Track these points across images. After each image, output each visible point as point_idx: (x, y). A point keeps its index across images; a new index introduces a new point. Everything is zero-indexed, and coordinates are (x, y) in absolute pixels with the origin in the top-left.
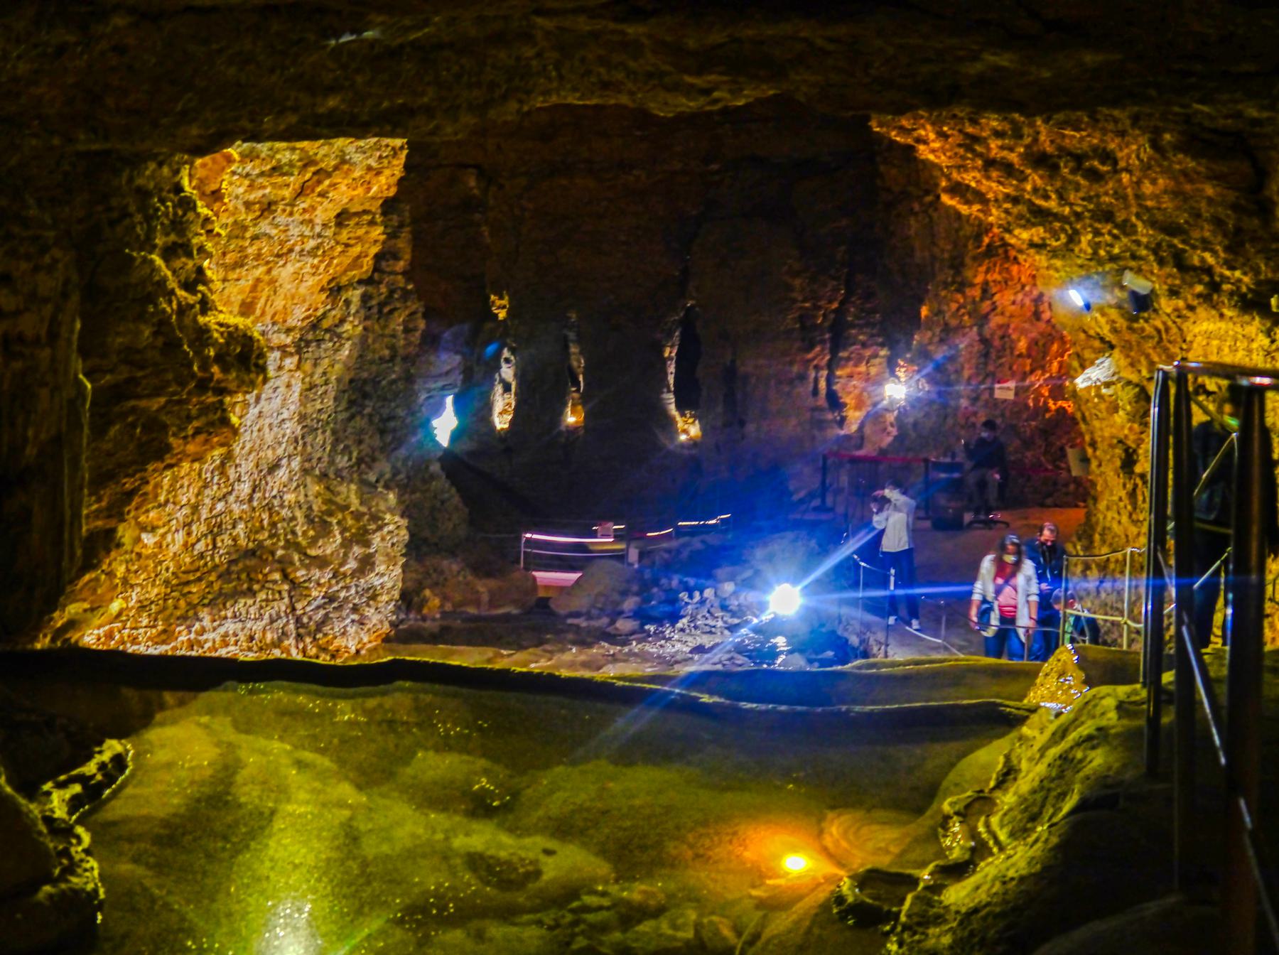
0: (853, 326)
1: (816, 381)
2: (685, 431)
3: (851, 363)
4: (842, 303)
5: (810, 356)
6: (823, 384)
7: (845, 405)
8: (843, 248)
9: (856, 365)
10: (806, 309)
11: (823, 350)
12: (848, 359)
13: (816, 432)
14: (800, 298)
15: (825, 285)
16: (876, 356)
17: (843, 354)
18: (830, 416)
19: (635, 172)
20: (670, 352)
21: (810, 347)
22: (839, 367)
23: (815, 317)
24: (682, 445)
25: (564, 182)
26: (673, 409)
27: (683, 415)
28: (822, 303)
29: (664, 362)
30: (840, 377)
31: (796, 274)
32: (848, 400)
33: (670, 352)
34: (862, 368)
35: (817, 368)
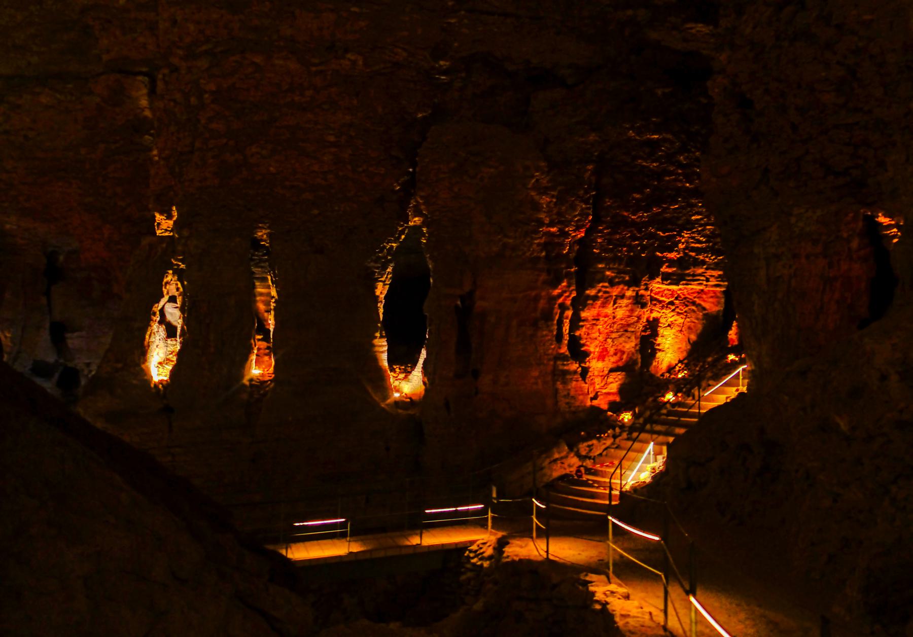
1: (560, 323)
3: (599, 302)
5: (557, 292)
6: (566, 328)
7: (587, 354)
8: (590, 167)
9: (604, 305)
10: (553, 235)
11: (569, 286)
12: (595, 298)
13: (559, 385)
14: (547, 221)
16: (623, 297)
17: (592, 292)
18: (575, 366)
19: (349, 56)
21: (555, 283)
22: (584, 306)
23: (562, 245)
24: (397, 403)
25: (258, 60)
30: (586, 320)
31: (544, 191)
32: (593, 348)
34: (609, 310)
35: (563, 307)
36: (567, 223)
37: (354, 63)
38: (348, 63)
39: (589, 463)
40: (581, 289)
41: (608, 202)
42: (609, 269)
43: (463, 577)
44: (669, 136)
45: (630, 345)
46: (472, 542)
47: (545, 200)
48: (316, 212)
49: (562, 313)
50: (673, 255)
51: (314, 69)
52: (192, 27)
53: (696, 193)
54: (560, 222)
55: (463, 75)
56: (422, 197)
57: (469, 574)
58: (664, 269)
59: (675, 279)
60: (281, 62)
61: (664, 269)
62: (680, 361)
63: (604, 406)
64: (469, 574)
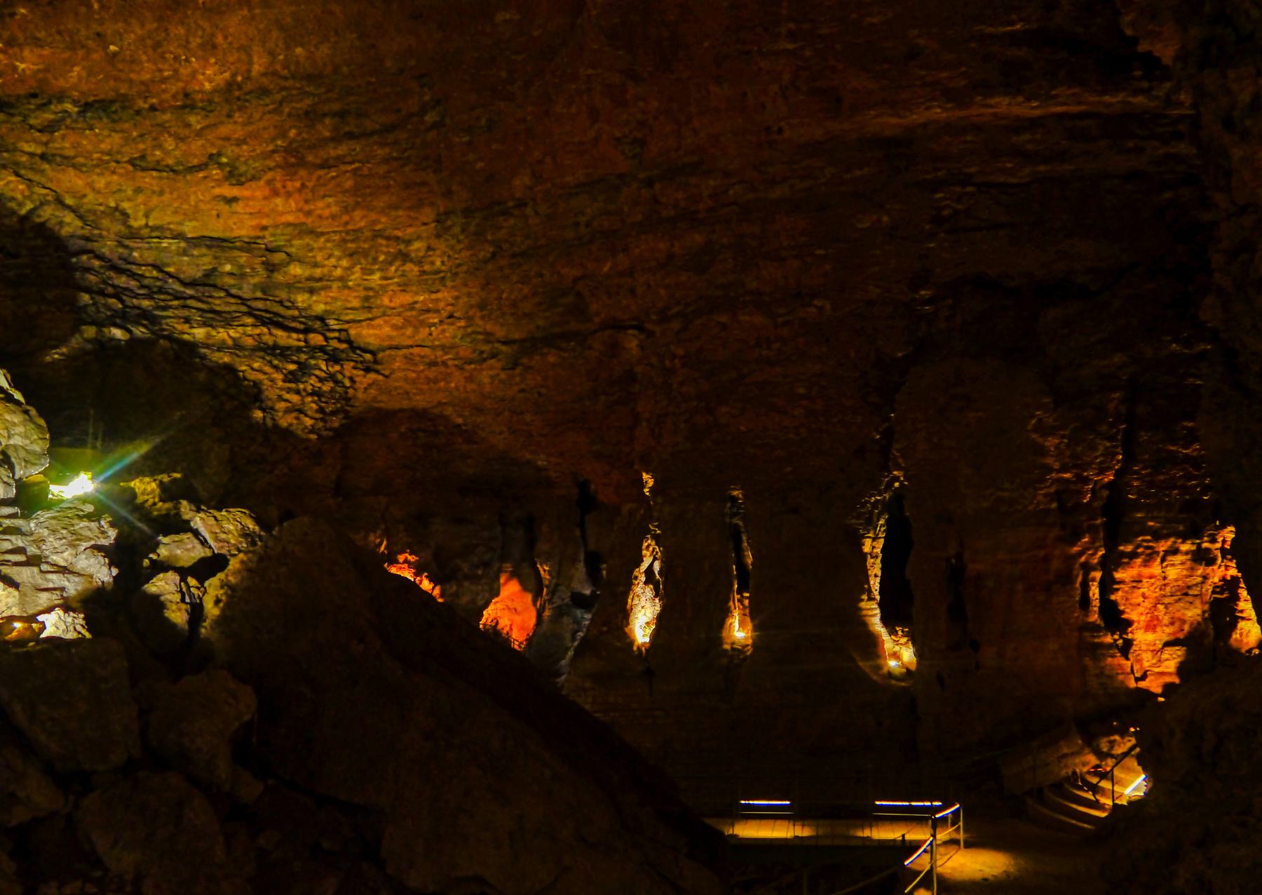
0: (1136, 506)
1: (1085, 587)
2: (896, 656)
3: (1139, 561)
4: (1118, 474)
5: (1076, 549)
6: (1095, 591)
7: (1129, 623)
8: (1117, 395)
9: (1146, 563)
10: (1067, 480)
11: (1093, 541)
12: (1134, 555)
13: (1088, 661)
14: (1057, 466)
15: (1093, 448)
16: (1175, 551)
19: (816, 302)
20: (873, 546)
21: (1075, 537)
22: (1118, 565)
23: (1081, 494)
25: (724, 319)
26: (876, 623)
27: (892, 632)
28: (1089, 473)
29: (864, 556)
30: (1122, 582)
33: (873, 546)
34: (1156, 569)
35: (1087, 568)
36: (1087, 466)
37: (821, 309)
38: (814, 310)
41: (1144, 436)
42: (1152, 519)
47: (1051, 442)
48: (789, 469)
49: (1086, 576)
52: (662, 292)
54: (1075, 466)
56: (898, 450)
60: (747, 318)
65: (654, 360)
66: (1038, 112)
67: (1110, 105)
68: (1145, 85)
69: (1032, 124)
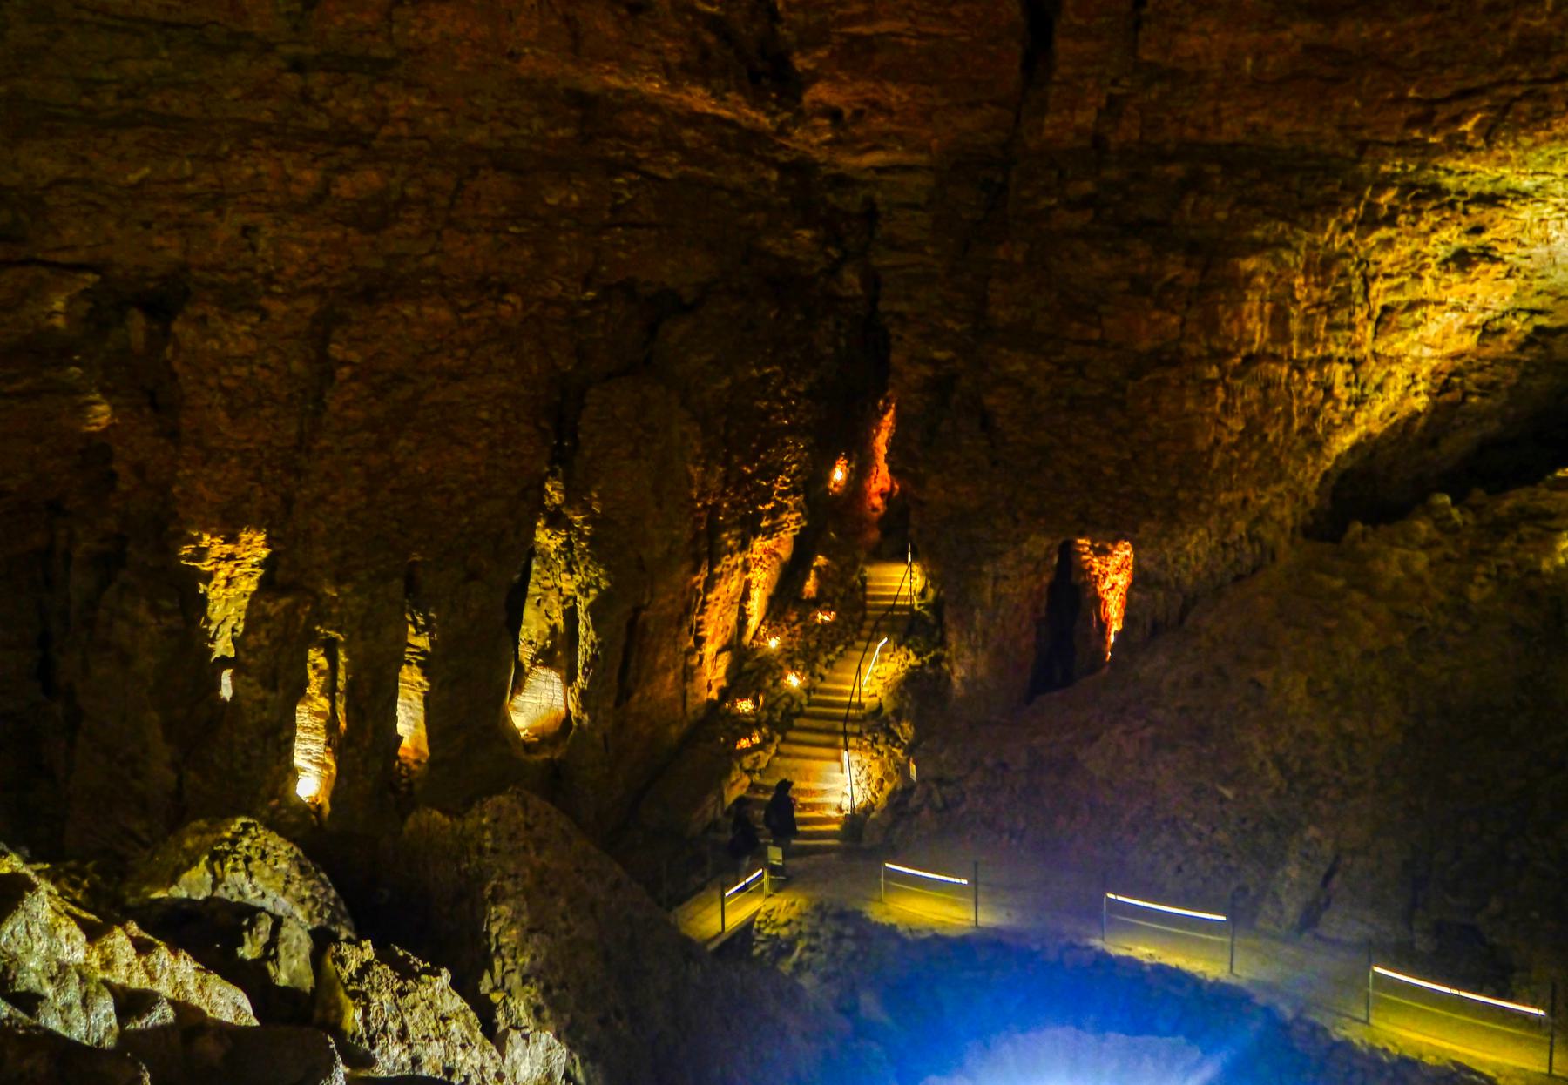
0: (724, 528)
16: (736, 567)
25: (408, 311)
35: (698, 595)
38: (509, 309)
39: (757, 778)
40: (710, 570)
42: (730, 537)
43: (756, 952)
44: (777, 368)
45: (732, 619)
46: (757, 912)
50: (768, 507)
51: (465, 317)
53: (790, 430)
55: (606, 307)
56: (599, 492)
57: (763, 947)
58: (765, 524)
59: (769, 533)
61: (765, 524)
62: (762, 623)
63: (716, 697)
64: (763, 947)
65: (272, 359)
66: (710, 110)
67: (747, 118)
68: (774, 107)
69: (696, 119)
